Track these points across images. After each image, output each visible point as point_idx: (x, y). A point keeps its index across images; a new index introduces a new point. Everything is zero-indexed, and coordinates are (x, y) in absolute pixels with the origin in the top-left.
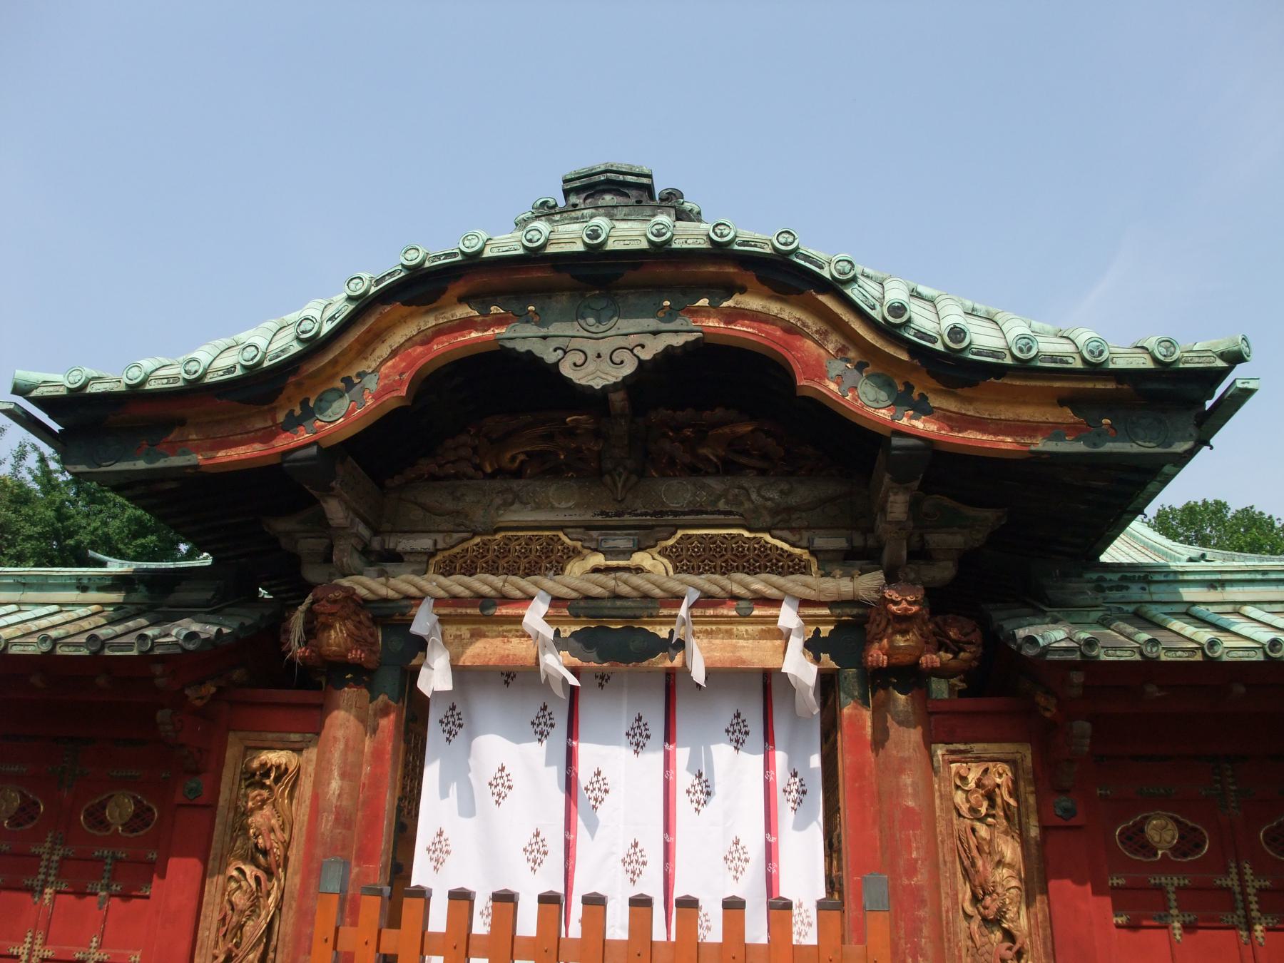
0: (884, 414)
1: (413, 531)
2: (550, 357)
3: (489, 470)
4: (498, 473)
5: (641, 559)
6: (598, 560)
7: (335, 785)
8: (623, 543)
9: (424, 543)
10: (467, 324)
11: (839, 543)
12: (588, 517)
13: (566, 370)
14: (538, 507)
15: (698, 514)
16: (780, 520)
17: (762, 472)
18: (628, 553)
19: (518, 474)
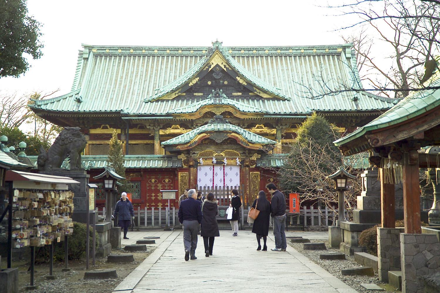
0: (245, 146)
1: (196, 151)
2: (214, 140)
3: (204, 143)
4: (205, 143)
5: (221, 154)
6: (217, 154)
7: (192, 177)
8: (219, 152)
9: (198, 152)
10: (206, 136)
11: (242, 152)
12: (216, 149)
13: (216, 141)
14: (210, 148)
15: (227, 149)
16: (236, 149)
17: (234, 144)
18: (220, 153)
19: (207, 144)
